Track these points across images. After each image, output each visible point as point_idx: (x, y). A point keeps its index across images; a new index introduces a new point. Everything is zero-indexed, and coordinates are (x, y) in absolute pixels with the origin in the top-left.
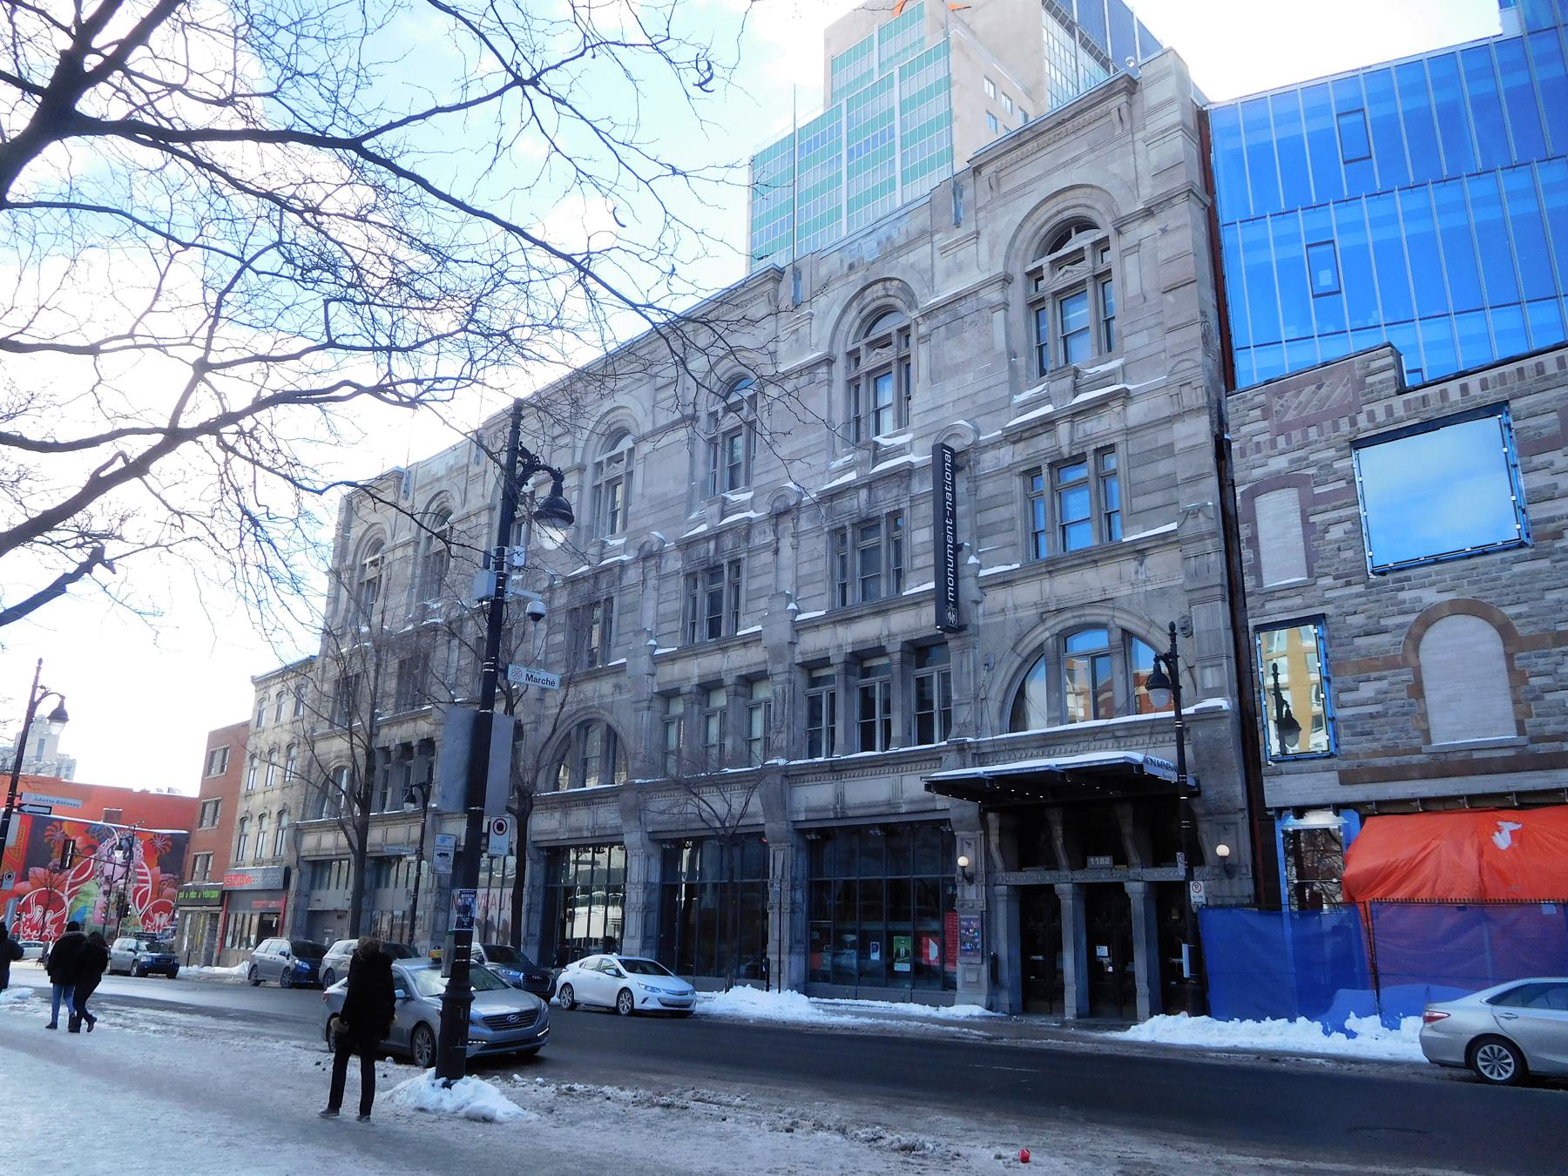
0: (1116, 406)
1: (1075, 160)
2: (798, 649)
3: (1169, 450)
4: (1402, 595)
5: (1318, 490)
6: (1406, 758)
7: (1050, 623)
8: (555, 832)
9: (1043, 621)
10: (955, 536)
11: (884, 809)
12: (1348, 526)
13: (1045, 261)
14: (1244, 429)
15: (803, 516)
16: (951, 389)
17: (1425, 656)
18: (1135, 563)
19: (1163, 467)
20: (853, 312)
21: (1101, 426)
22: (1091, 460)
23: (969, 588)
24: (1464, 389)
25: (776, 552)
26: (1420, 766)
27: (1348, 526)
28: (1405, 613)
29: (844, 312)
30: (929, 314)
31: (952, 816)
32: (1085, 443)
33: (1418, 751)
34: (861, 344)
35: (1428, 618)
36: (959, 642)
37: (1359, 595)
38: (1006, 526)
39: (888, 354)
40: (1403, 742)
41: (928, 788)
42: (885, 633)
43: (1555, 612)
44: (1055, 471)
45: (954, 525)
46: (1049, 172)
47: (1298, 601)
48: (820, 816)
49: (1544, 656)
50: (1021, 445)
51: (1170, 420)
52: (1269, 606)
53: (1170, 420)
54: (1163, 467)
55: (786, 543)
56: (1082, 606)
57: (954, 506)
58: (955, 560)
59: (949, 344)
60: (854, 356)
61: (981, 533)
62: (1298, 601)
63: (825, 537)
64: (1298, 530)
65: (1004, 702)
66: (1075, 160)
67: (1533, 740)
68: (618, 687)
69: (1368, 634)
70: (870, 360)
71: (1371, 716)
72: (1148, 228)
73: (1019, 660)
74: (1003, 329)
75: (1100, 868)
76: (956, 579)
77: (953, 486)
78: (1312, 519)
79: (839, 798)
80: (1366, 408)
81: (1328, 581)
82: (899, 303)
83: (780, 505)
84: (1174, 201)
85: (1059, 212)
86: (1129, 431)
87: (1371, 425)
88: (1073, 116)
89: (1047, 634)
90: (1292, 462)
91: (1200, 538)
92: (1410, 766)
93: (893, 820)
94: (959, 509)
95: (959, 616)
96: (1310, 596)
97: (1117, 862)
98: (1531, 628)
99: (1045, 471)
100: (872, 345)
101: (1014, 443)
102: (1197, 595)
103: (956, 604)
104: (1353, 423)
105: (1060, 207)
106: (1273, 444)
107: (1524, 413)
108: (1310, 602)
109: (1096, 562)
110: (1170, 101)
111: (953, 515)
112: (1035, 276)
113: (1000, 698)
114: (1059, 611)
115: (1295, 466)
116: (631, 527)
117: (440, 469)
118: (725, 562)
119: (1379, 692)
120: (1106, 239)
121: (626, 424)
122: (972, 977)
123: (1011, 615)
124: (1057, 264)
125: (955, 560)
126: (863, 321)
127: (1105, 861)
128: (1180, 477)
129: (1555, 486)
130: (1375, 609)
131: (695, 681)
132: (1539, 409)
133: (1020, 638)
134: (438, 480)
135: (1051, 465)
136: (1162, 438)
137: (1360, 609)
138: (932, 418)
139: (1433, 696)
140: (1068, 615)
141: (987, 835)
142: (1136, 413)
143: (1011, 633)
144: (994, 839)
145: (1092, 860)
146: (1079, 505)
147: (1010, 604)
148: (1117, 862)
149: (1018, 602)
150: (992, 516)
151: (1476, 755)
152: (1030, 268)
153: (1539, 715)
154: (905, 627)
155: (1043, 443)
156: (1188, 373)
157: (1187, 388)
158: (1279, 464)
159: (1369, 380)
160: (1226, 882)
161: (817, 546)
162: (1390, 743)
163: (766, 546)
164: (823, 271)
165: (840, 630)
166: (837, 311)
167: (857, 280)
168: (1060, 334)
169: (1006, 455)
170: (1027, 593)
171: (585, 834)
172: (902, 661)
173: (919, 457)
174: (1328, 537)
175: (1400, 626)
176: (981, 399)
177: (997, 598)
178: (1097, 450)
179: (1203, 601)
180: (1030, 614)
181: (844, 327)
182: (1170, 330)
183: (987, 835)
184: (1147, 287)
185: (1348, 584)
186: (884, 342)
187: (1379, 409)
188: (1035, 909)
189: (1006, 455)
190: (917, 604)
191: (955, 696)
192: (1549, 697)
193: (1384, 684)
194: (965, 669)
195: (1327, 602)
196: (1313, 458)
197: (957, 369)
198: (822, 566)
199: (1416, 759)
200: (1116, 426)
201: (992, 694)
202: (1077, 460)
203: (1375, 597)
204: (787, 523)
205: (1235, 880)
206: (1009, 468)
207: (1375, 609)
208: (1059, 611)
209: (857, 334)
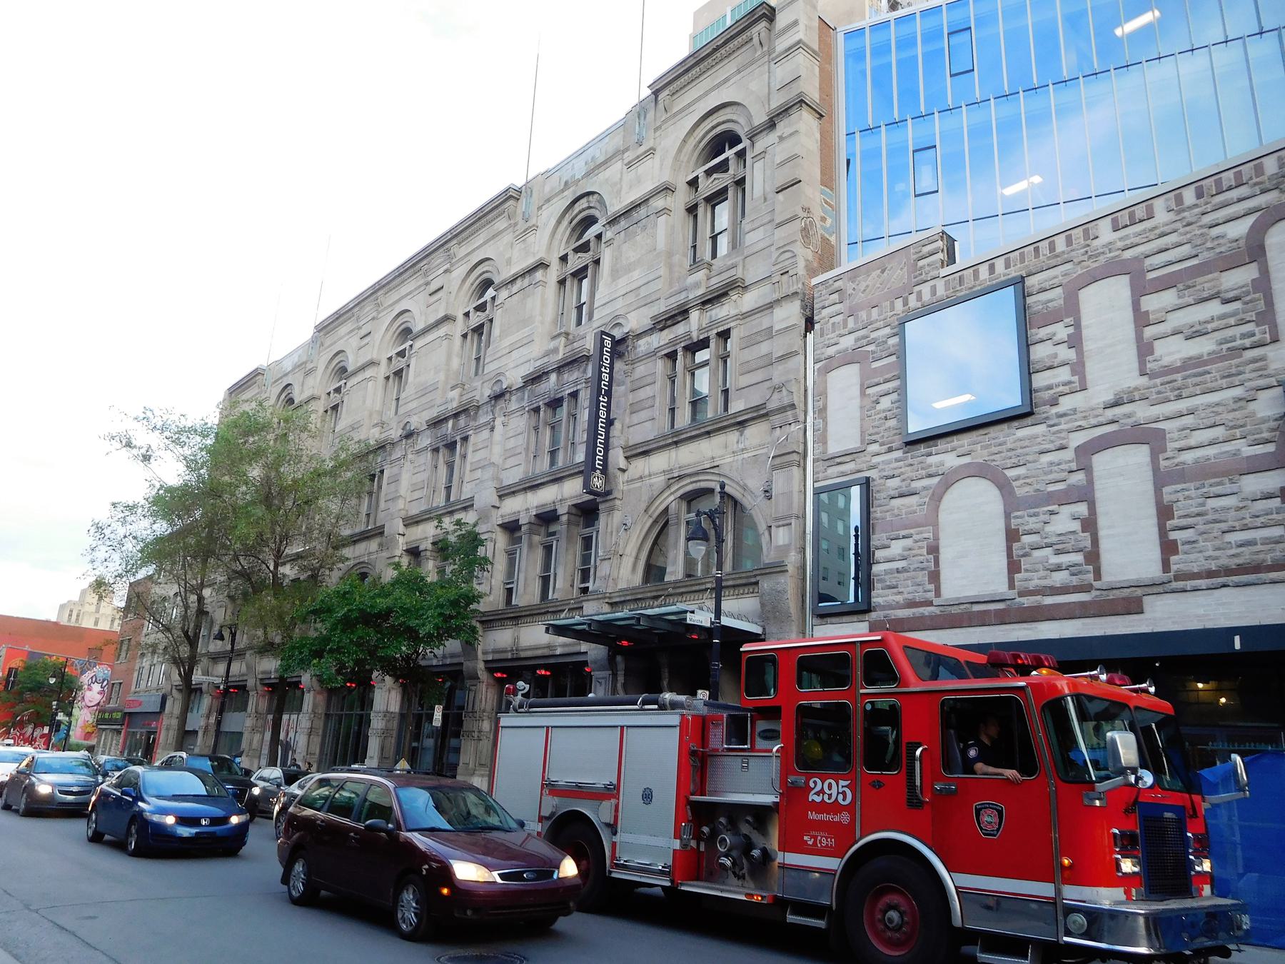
0: (734, 296)
1: (726, 80)
2: (501, 512)
3: (769, 333)
4: (931, 460)
5: (875, 365)
6: (921, 610)
9: (669, 487)
10: (608, 412)
11: (546, 652)
12: (894, 396)
14: (825, 312)
15: (514, 398)
16: (623, 284)
17: (943, 517)
19: (764, 348)
20: (565, 222)
21: (722, 311)
22: (712, 344)
23: (617, 457)
24: (992, 269)
25: (492, 429)
26: (932, 617)
27: (894, 396)
28: (930, 476)
29: (559, 222)
30: (613, 222)
31: (589, 658)
32: (709, 328)
33: (930, 604)
34: (569, 251)
35: (949, 480)
37: (897, 460)
38: (650, 403)
39: (585, 258)
40: (919, 596)
41: (547, 631)
43: (1045, 474)
44: (689, 355)
45: (609, 403)
46: (706, 94)
49: (1035, 515)
50: (666, 332)
51: (770, 306)
53: (770, 306)
54: (764, 348)
55: (498, 422)
56: (697, 474)
57: (610, 385)
58: (607, 433)
59: (625, 247)
60: (564, 259)
61: (635, 408)
63: (526, 415)
64: (857, 402)
65: (637, 558)
66: (726, 80)
67: (1021, 594)
68: (380, 545)
69: (901, 496)
70: (576, 262)
71: (898, 571)
72: (772, 137)
73: (651, 521)
74: (667, 229)
76: (606, 449)
77: (612, 368)
78: (869, 391)
79: (516, 639)
80: (917, 289)
81: (874, 448)
82: (596, 213)
83: (497, 389)
84: (791, 112)
85: (714, 128)
87: (919, 304)
88: (725, 43)
89: (672, 498)
90: (857, 340)
92: (922, 617)
93: (552, 661)
94: (617, 390)
95: (607, 481)
96: (861, 462)
98: (1027, 489)
99: (680, 354)
100: (576, 250)
101: (662, 330)
102: (778, 461)
103: (604, 471)
104: (906, 303)
105: (715, 122)
106: (845, 322)
107: (1035, 290)
108: (859, 467)
110: (795, 23)
111: (609, 394)
112: (693, 183)
113: (634, 554)
114: (680, 477)
115: (859, 344)
116: (401, 411)
117: (288, 366)
118: (458, 438)
119: (905, 549)
120: (744, 150)
121: (409, 325)
124: (709, 173)
125: (607, 433)
126: (573, 230)
128: (775, 356)
129: (1055, 356)
130: (909, 472)
131: (431, 540)
132: (1047, 285)
134: (286, 375)
135: (686, 348)
136: (764, 321)
137: (896, 472)
138: (607, 310)
139: (945, 555)
141: (615, 675)
142: (749, 300)
144: (621, 679)
146: (703, 382)
150: (642, 394)
151: (976, 608)
152: (690, 177)
153: (1027, 571)
155: (680, 329)
156: (787, 263)
157: (786, 276)
158: (848, 342)
159: (921, 263)
161: (520, 423)
162: (910, 596)
163: (485, 424)
164: (547, 189)
165: (530, 495)
166: (553, 222)
167: (570, 196)
168: (708, 234)
169: (660, 340)
170: (659, 462)
172: (569, 522)
173: (589, 344)
174: (879, 407)
175: (925, 488)
176: (643, 292)
177: (639, 466)
178: (718, 334)
180: (660, 481)
181: (558, 236)
182: (780, 225)
183: (615, 675)
184: (768, 189)
185: (890, 450)
186: (584, 248)
187: (925, 289)
189: (660, 340)
192: (1036, 553)
193: (908, 542)
195: (873, 467)
196: (873, 335)
197: (629, 269)
198: (521, 441)
199: (926, 611)
200: (733, 312)
201: (628, 551)
202: (704, 344)
203: (910, 461)
204: (501, 403)
206: (654, 353)
207: (909, 472)
208: (680, 477)
209: (567, 242)
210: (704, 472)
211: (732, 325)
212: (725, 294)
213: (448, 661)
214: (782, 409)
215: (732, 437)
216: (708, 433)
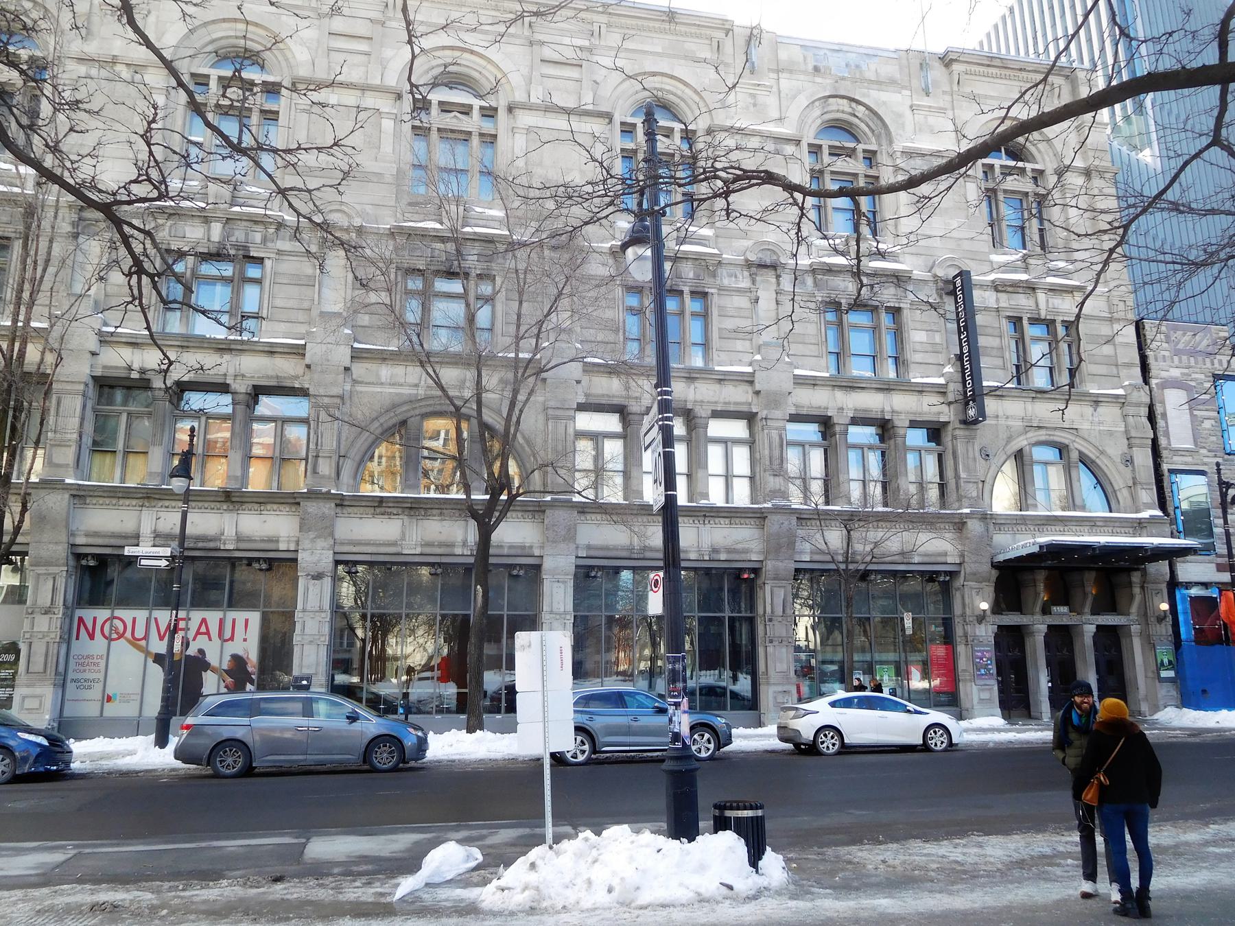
7: (1030, 435)
8: (394, 544)
18: (1092, 409)
36: (967, 433)
47: (1189, 459)
48: (933, 560)
52: (1175, 458)
62: (1189, 459)
75: (1061, 615)
81: (1204, 451)
89: (1025, 443)
91: (1138, 405)
122: (985, 695)
123: (1002, 422)
127: (1065, 609)
133: (1010, 439)
140: (1043, 432)
143: (1003, 435)
145: (1054, 609)
147: (1001, 414)
149: (896, 408)
157: (1122, 304)
165: (839, 394)
171: (458, 551)
188: (1011, 644)
190: (921, 392)
191: (963, 475)
194: (971, 455)
196: (1194, 376)
213: (723, 557)
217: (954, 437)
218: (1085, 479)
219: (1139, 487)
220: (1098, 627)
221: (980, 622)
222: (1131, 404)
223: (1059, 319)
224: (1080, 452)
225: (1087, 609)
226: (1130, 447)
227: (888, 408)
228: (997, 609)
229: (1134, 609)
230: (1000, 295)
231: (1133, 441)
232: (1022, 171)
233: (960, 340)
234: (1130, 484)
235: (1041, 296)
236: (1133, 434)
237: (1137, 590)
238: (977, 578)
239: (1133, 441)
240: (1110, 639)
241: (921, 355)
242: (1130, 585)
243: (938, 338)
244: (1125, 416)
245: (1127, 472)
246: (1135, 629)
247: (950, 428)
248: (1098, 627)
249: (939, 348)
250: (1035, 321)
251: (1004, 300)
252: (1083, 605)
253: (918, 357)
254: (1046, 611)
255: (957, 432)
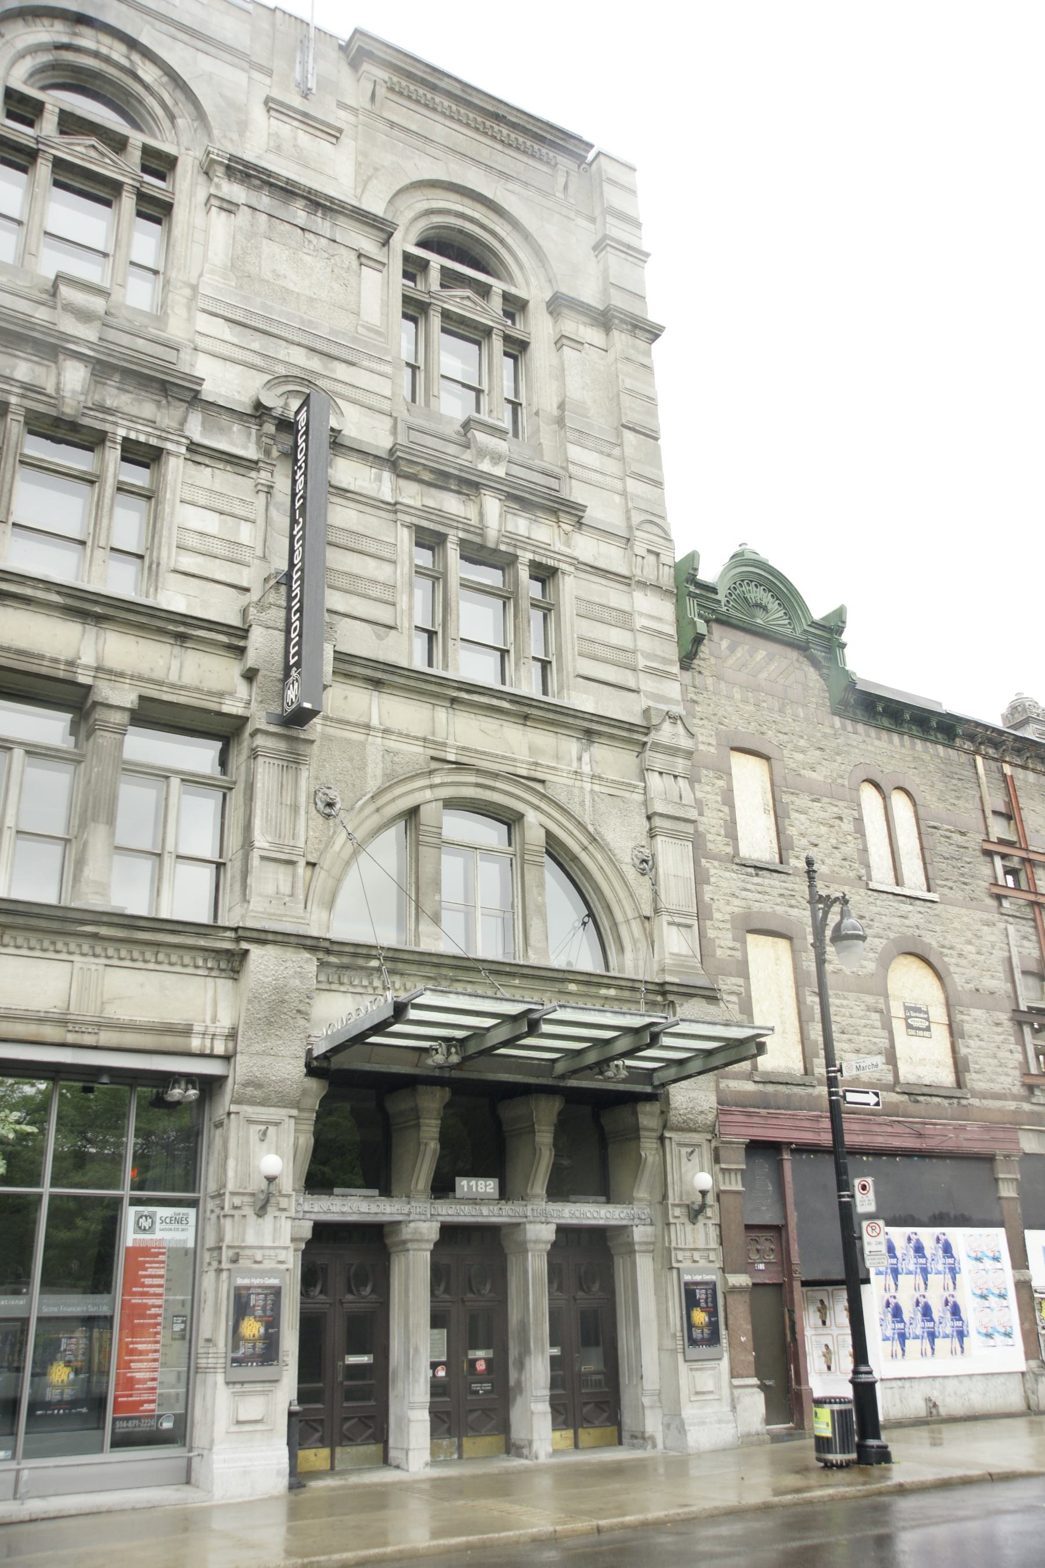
9: (431, 773)
13: (436, 261)
42: (88, 658)
56: (495, 775)
73: (375, 820)
75: (477, 1198)
86: (580, 566)
89: (428, 794)
97: (504, 1194)
109: (526, 717)
114: (460, 766)
127: (488, 1186)
142: (586, 547)
145: (465, 1185)
147: (375, 722)
148: (504, 1194)
154: (144, 669)
155: (451, 504)
157: (652, 558)
160: (689, 1227)
179: (674, 835)
205: (700, 1225)
206: (394, 507)
208: (460, 766)
210: (514, 778)
211: (563, 566)
212: (555, 512)
214: (673, 751)
215: (571, 746)
216: (526, 717)
217: (254, 754)
218: (554, 886)
219: (665, 918)
220: (561, 1229)
221: (261, 1211)
222: (657, 746)
223: (525, 557)
224: (549, 834)
225: (540, 1186)
226: (652, 834)
227: (88, 658)
228: (318, 1180)
229: (642, 1193)
230: (402, 482)
231: (657, 822)
232: (484, 291)
233: (292, 537)
234: (648, 911)
235: (492, 505)
236: (659, 807)
237: (648, 1148)
238: (262, 1094)
239: (657, 822)
240: (590, 1262)
241: (200, 559)
242: (634, 1133)
243: (246, 534)
244: (643, 772)
245: (643, 889)
246: (640, 1234)
247: (249, 729)
248: (561, 1229)
249: (246, 556)
250: (476, 553)
251: (412, 494)
252: (528, 1178)
253: (189, 562)
254: (442, 1188)
255: (260, 741)
